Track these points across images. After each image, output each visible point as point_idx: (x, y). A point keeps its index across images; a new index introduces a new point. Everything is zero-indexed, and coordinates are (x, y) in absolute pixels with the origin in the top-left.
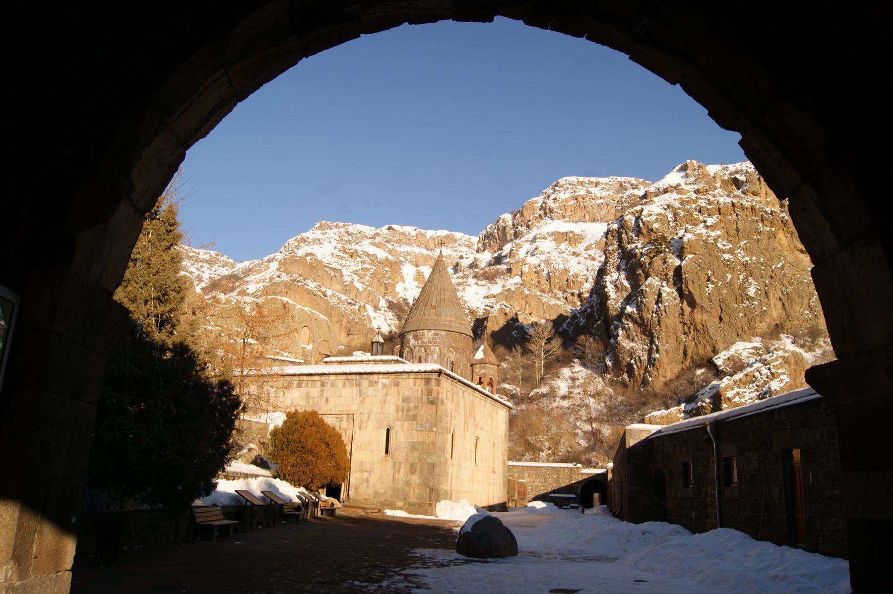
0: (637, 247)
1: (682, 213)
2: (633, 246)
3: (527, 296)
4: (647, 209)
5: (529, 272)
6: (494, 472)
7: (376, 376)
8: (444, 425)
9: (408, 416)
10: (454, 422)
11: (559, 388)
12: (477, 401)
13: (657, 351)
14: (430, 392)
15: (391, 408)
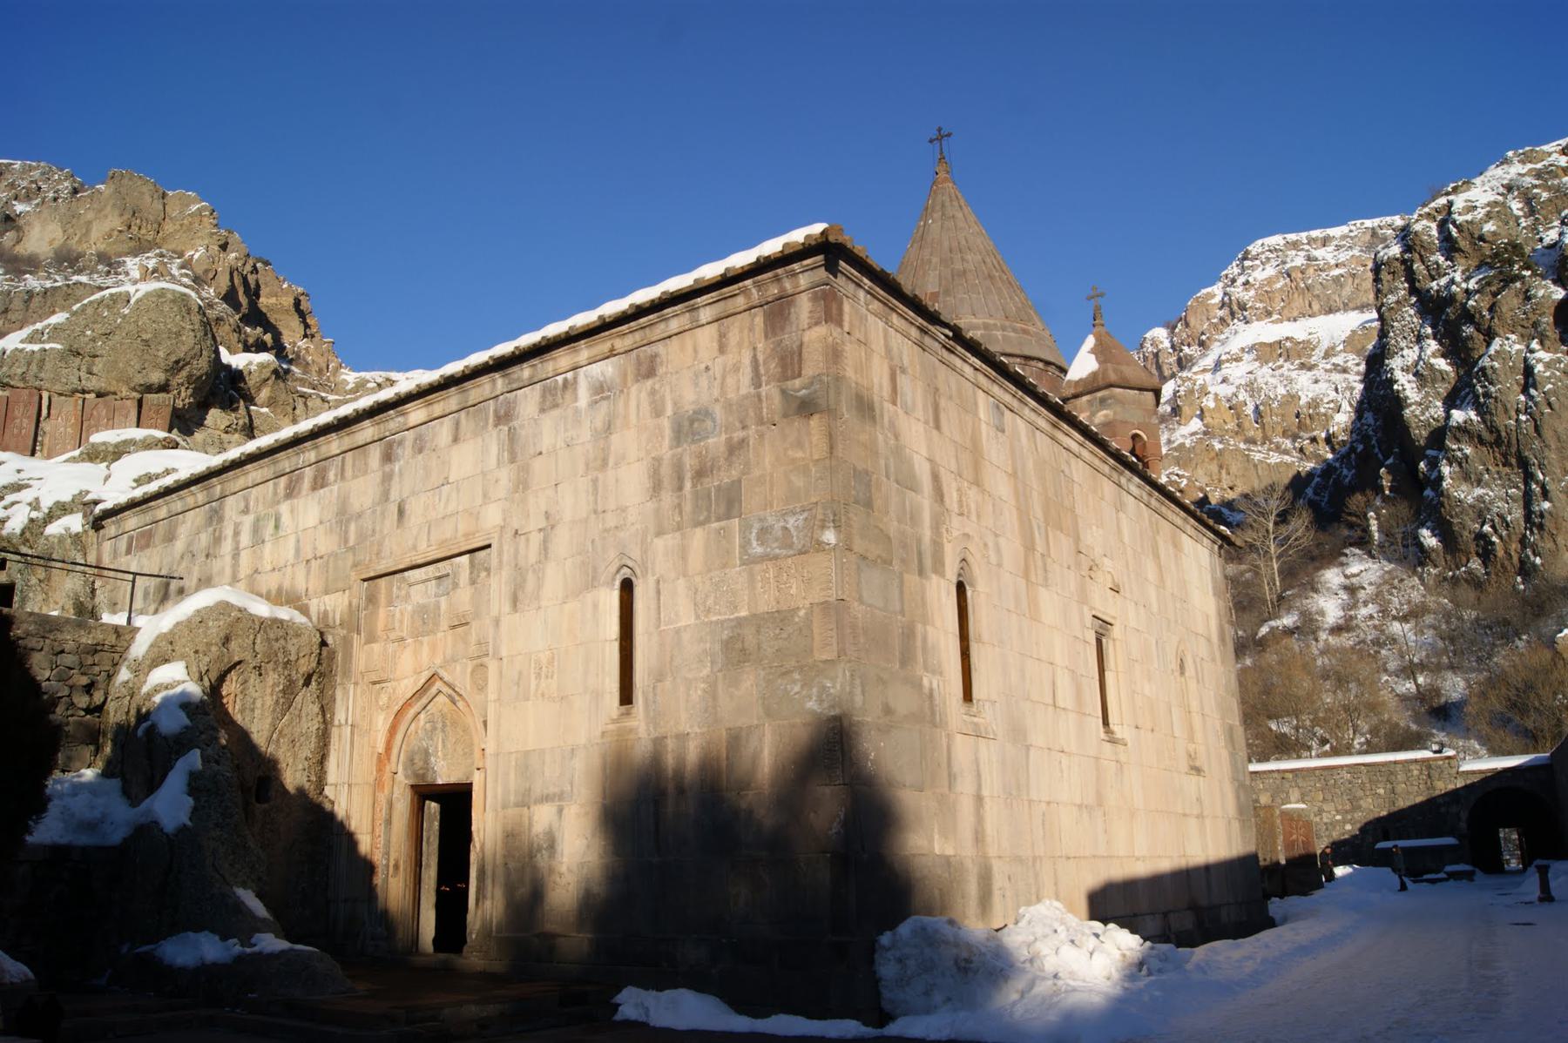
0: (1452, 281)
1: (1545, 195)
2: (1443, 281)
3: (1220, 453)
4: (1459, 202)
5: (1217, 408)
6: (1197, 770)
7: (562, 359)
8: (893, 527)
9: (701, 498)
10: (956, 525)
11: (1322, 613)
12: (1078, 471)
13: (1545, 494)
14: (790, 362)
15: (630, 482)
